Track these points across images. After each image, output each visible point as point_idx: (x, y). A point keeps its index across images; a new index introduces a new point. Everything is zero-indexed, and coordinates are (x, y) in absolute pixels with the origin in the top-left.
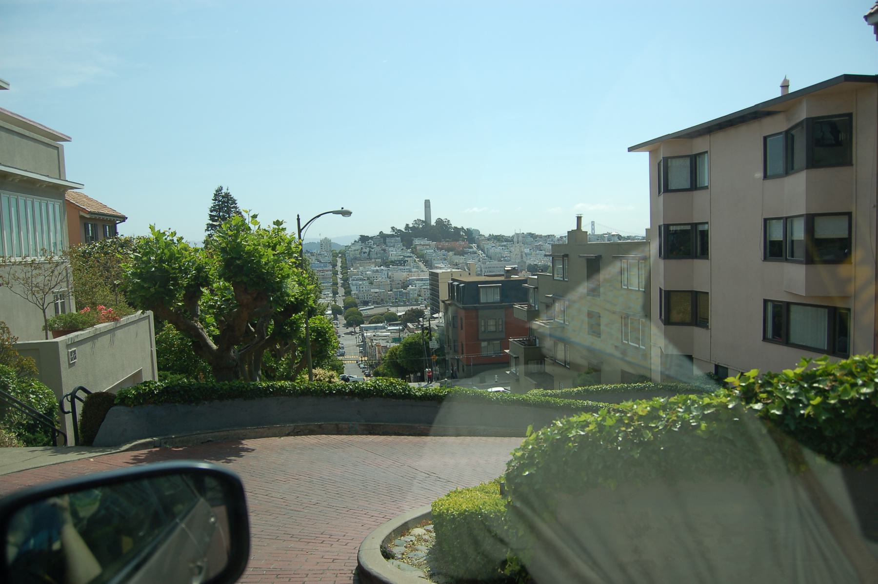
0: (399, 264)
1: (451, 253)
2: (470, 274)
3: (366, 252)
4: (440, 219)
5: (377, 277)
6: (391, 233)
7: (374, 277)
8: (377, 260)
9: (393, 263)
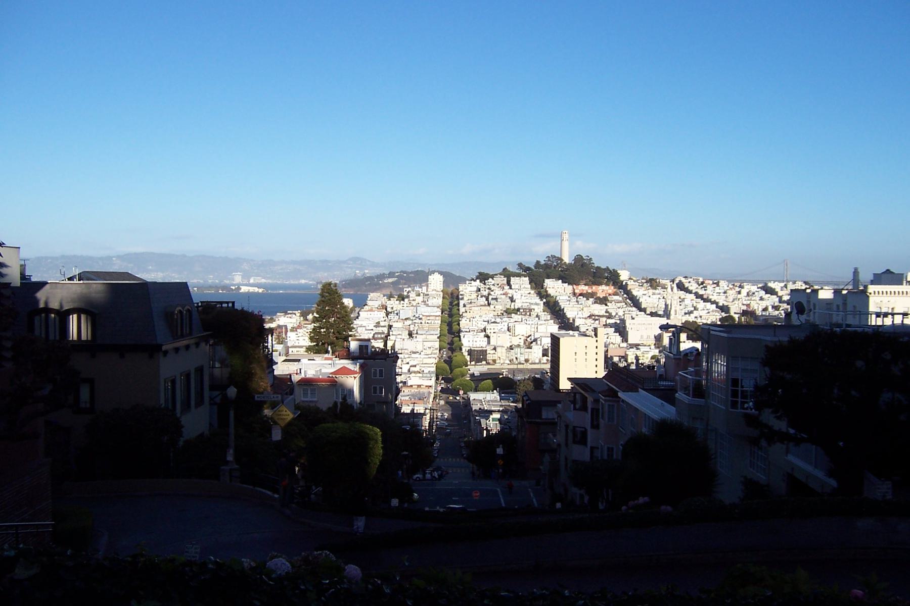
1: (591, 300)
2: (597, 341)
3: (485, 296)
5: (494, 329)
6: (518, 271)
7: (490, 329)
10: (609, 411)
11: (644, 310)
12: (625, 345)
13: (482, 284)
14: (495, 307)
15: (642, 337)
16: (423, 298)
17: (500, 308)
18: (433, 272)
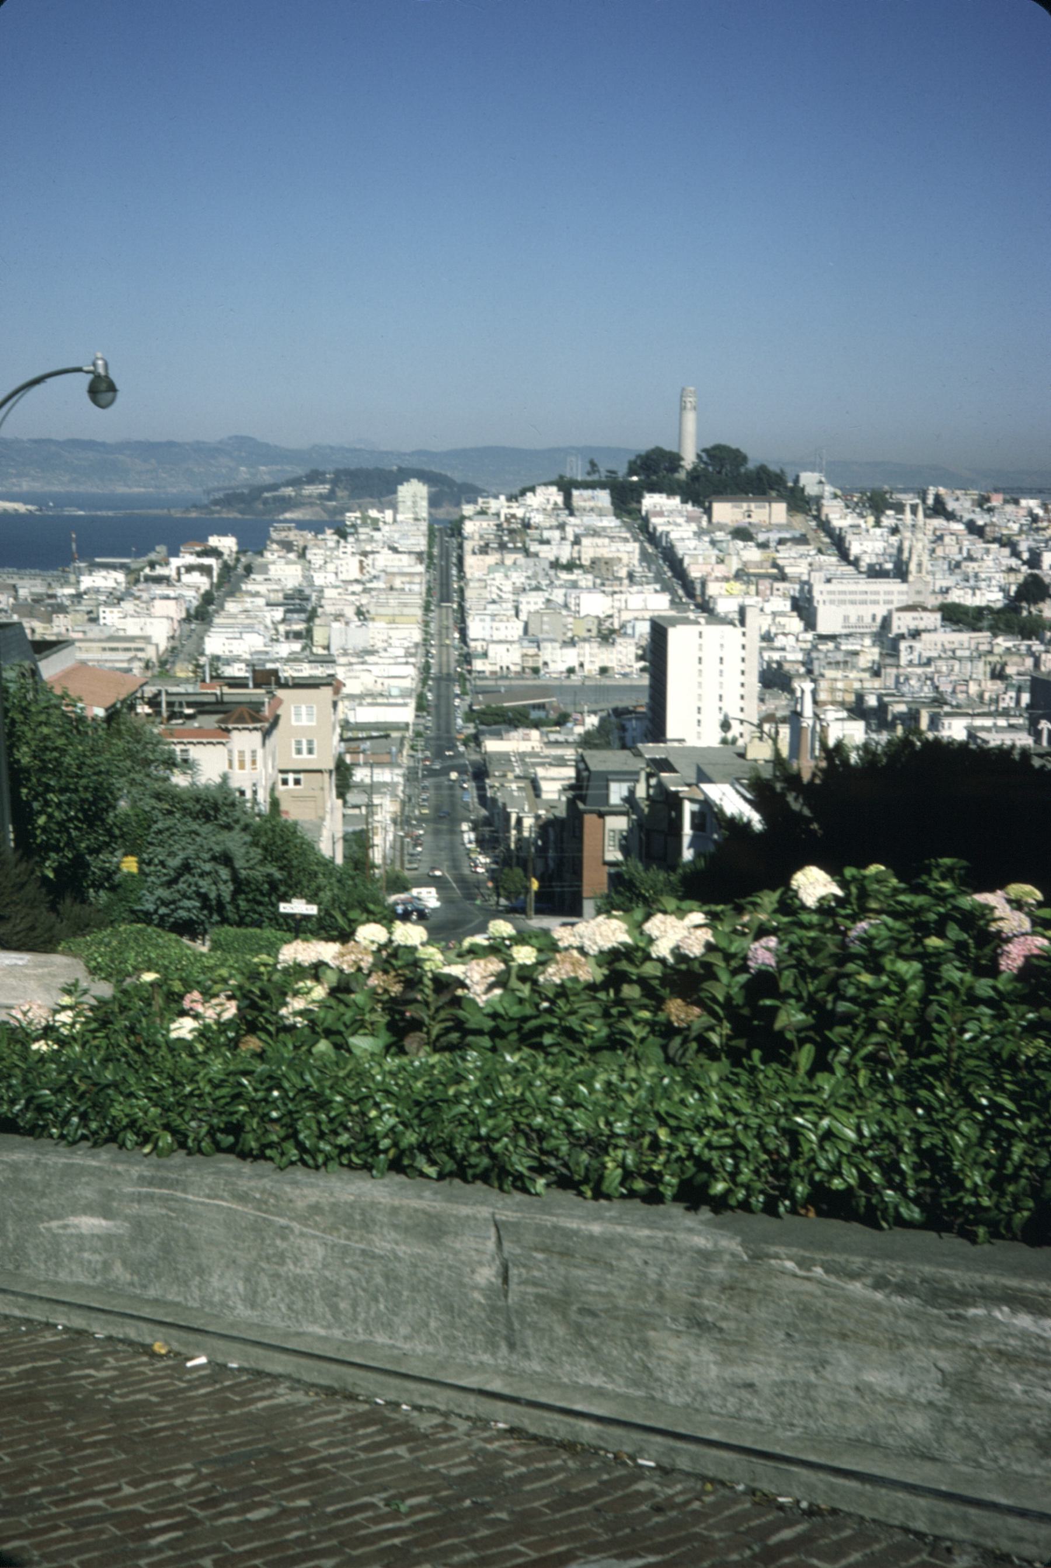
11: (855, 563)
12: (809, 636)
15: (846, 618)
18: (404, 475)
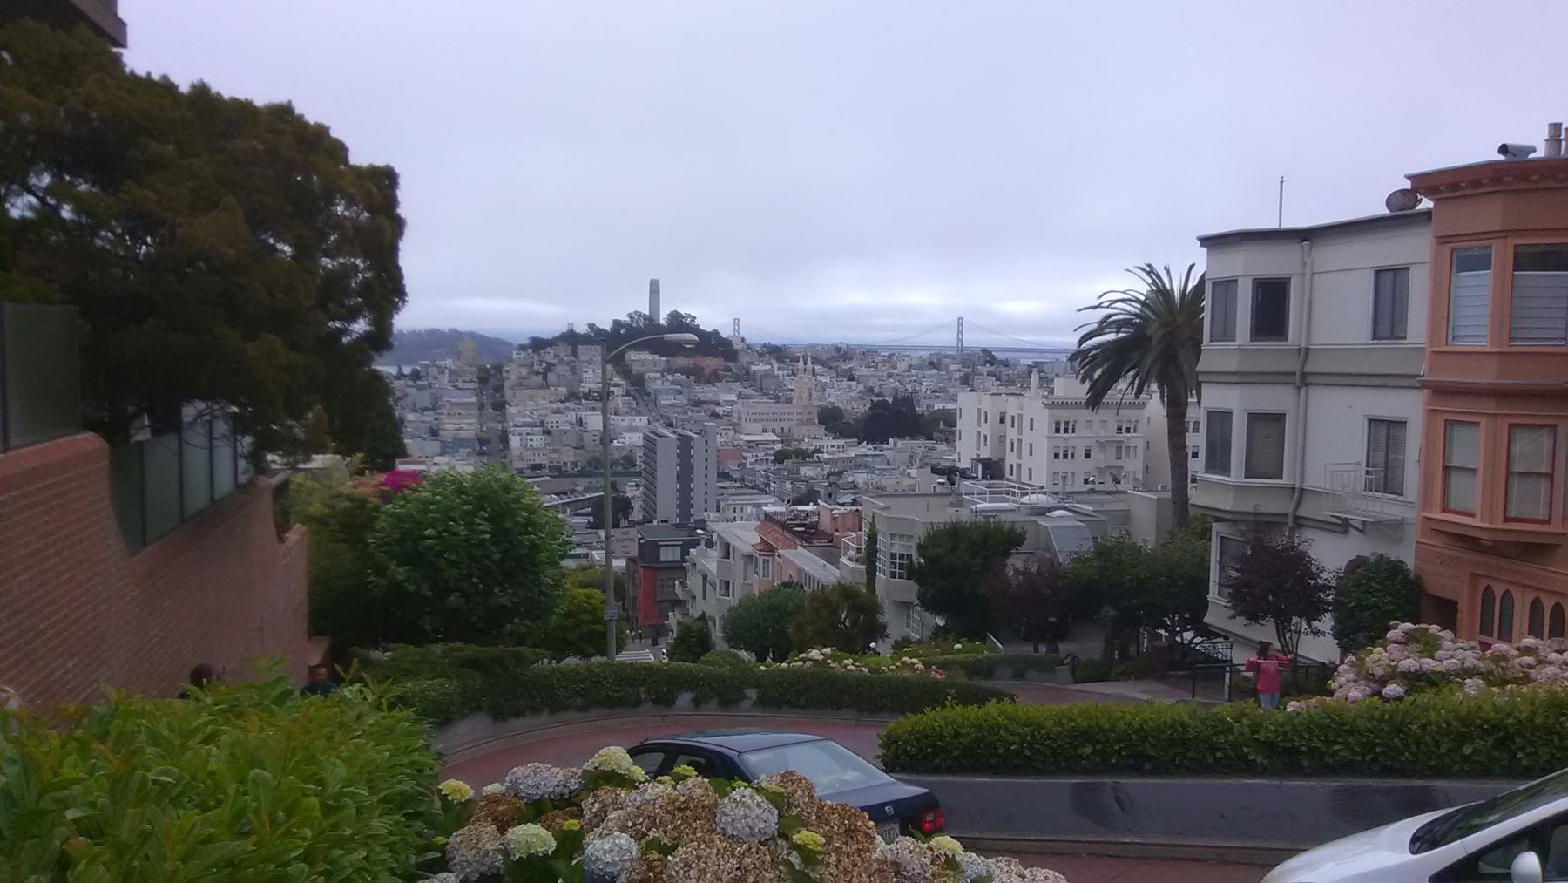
0: (598, 398)
4: (676, 311)
5: (557, 422)
7: (552, 422)
8: (559, 389)
9: (587, 396)
10: (764, 567)
13: (536, 357)
14: (556, 390)
16: (449, 375)
17: (564, 389)
